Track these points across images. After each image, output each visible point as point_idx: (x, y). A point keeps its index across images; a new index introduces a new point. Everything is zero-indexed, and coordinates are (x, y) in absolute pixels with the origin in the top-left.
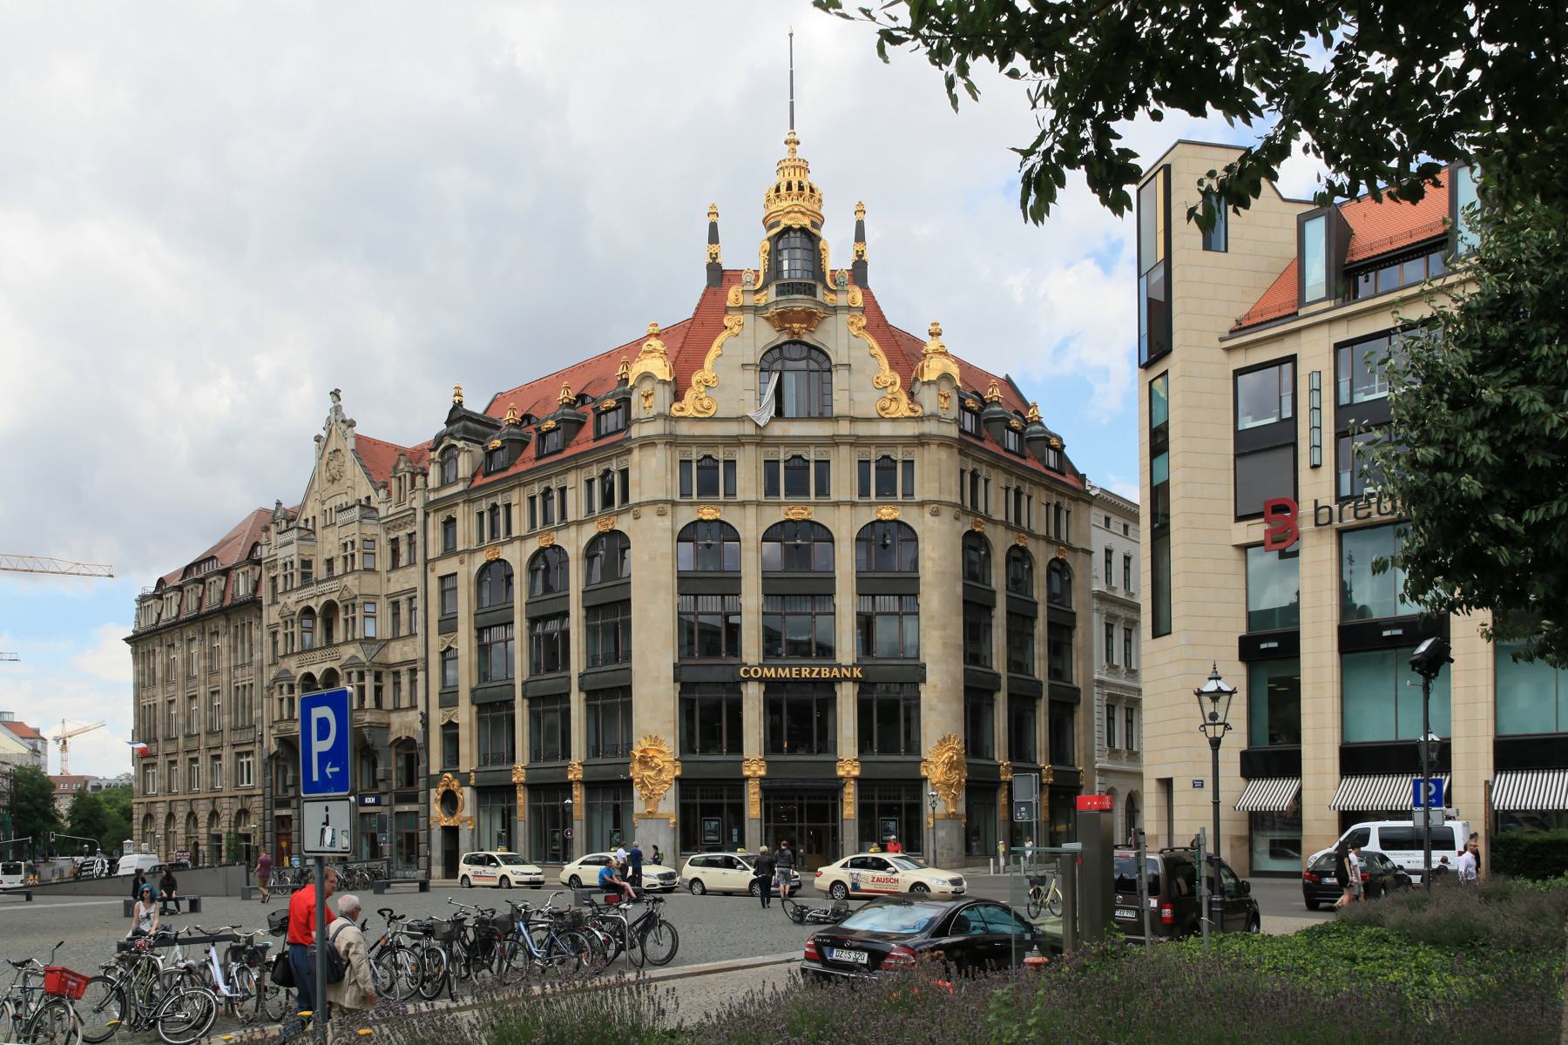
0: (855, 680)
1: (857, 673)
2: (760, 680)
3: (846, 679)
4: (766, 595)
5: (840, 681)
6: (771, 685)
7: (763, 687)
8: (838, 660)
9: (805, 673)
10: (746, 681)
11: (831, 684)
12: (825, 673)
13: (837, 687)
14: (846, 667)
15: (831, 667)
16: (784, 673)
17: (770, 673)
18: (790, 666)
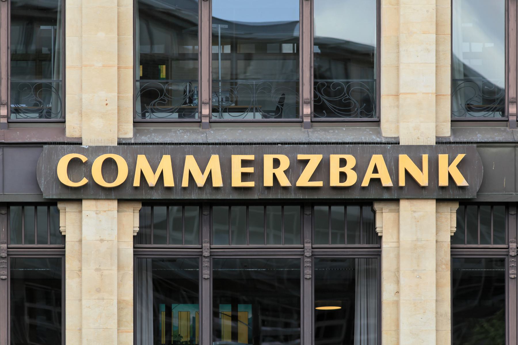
0: (443, 196)
1: (449, 170)
2: (123, 196)
3: (413, 190)
4: (196, 25)
5: (393, 197)
6: (161, 212)
7: (131, 220)
8: (387, 130)
9: (275, 172)
10: (75, 197)
11: (355, 213)
12: (343, 172)
13: (384, 220)
14: (415, 152)
15: (363, 150)
16: (204, 172)
17: (157, 172)
18: (225, 149)
